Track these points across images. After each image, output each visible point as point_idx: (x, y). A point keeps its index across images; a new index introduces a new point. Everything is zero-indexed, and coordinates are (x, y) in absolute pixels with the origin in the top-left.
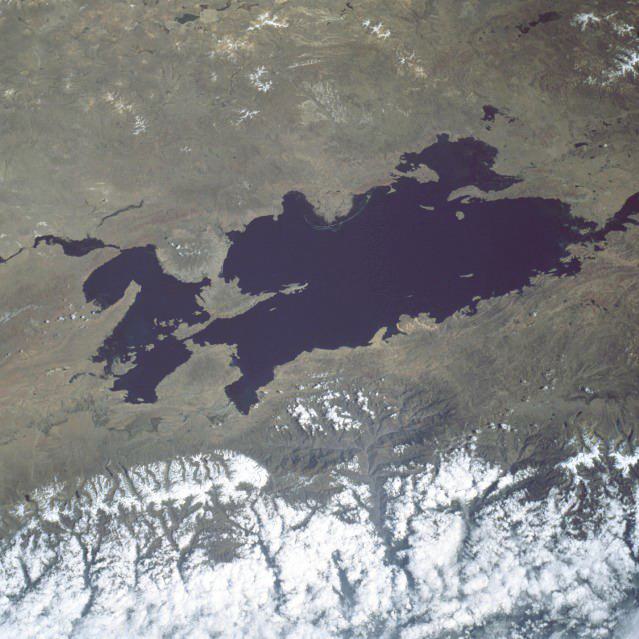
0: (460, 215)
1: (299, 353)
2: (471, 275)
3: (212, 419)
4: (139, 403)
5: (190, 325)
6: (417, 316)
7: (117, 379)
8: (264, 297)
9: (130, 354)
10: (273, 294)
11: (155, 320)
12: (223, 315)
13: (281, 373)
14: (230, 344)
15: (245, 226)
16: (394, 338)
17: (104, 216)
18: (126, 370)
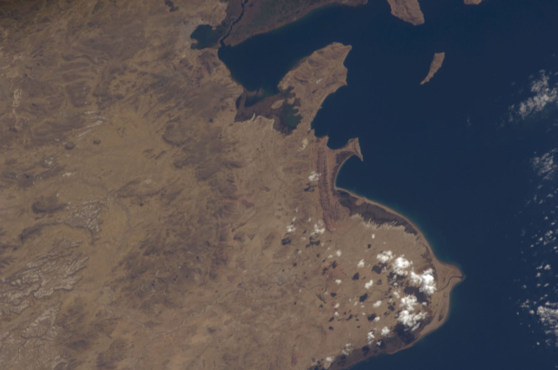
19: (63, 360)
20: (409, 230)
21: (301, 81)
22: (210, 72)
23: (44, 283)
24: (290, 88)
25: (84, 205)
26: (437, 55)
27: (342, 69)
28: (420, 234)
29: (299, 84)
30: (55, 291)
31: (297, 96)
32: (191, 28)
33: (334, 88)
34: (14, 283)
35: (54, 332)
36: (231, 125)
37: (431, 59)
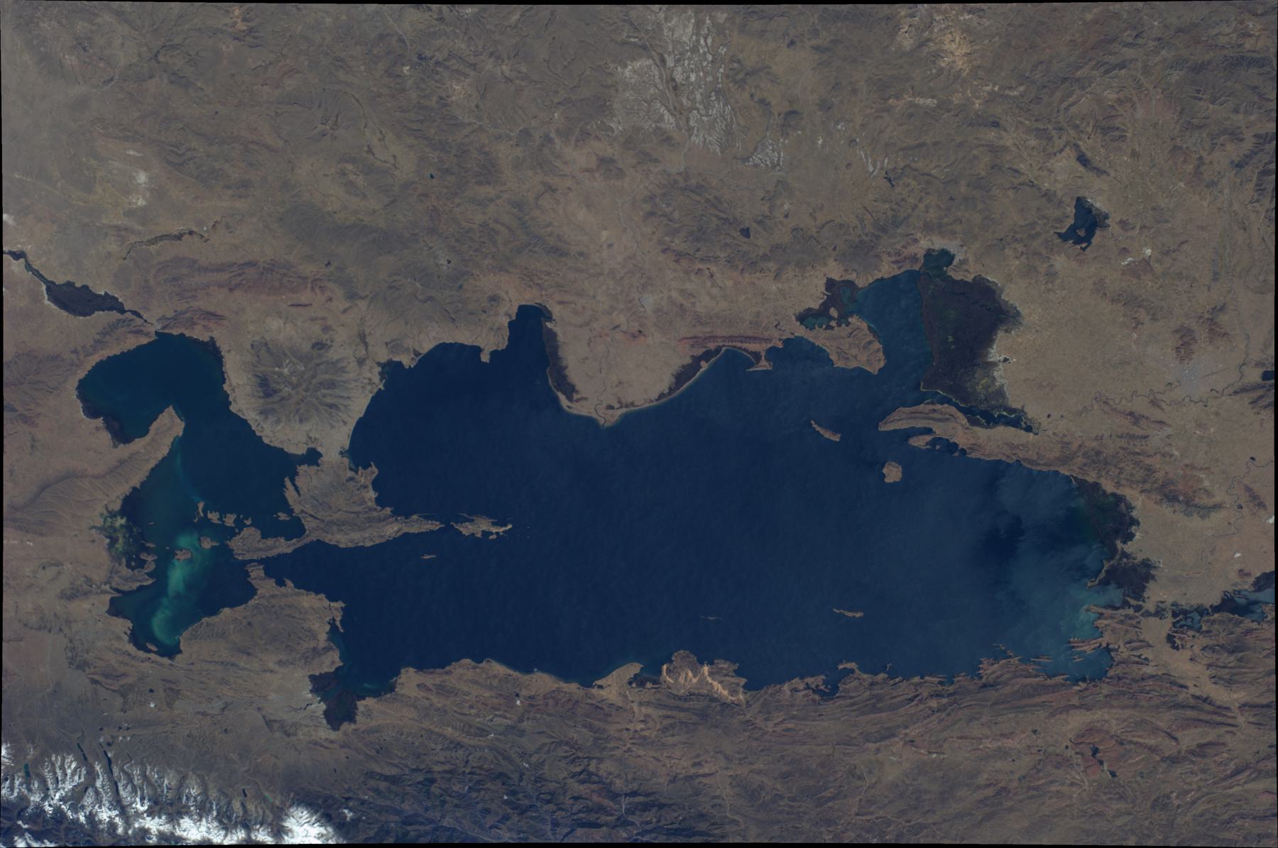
0: (893, 473)
1: (458, 659)
2: (858, 615)
3: (269, 723)
4: (150, 651)
5: (264, 536)
6: (711, 663)
7: (117, 595)
8: (418, 525)
9: (144, 556)
10: (434, 526)
11: (201, 506)
12: (330, 538)
13: (409, 680)
14: (332, 598)
15: (417, 353)
16: (648, 692)
17: (133, 239)
18: (135, 586)
19: (616, 133)
20: (661, 396)
21: (851, 333)
22: (893, 262)
23: (705, 118)
24: (848, 324)
25: (779, 154)
26: (839, 435)
27: (852, 365)
28: (655, 403)
29: (850, 331)
30: (693, 128)
31: (836, 328)
32: (952, 251)
33: (833, 357)
34: (713, 94)
35: (648, 125)
36: (825, 275)
37: (835, 431)
